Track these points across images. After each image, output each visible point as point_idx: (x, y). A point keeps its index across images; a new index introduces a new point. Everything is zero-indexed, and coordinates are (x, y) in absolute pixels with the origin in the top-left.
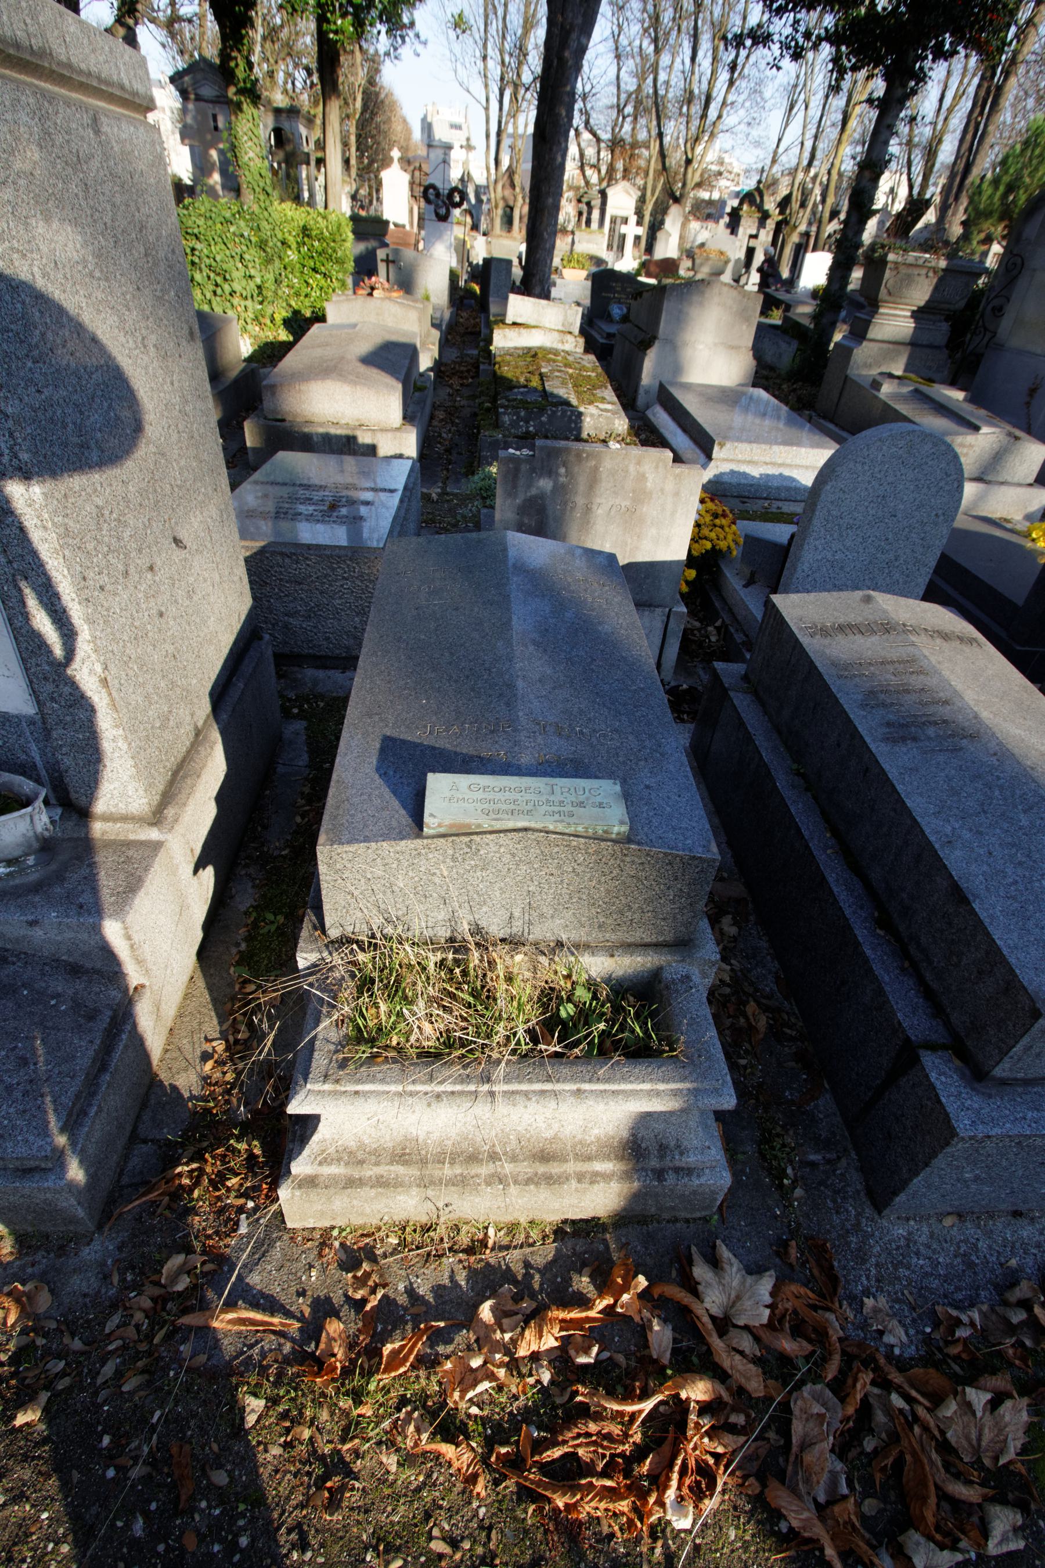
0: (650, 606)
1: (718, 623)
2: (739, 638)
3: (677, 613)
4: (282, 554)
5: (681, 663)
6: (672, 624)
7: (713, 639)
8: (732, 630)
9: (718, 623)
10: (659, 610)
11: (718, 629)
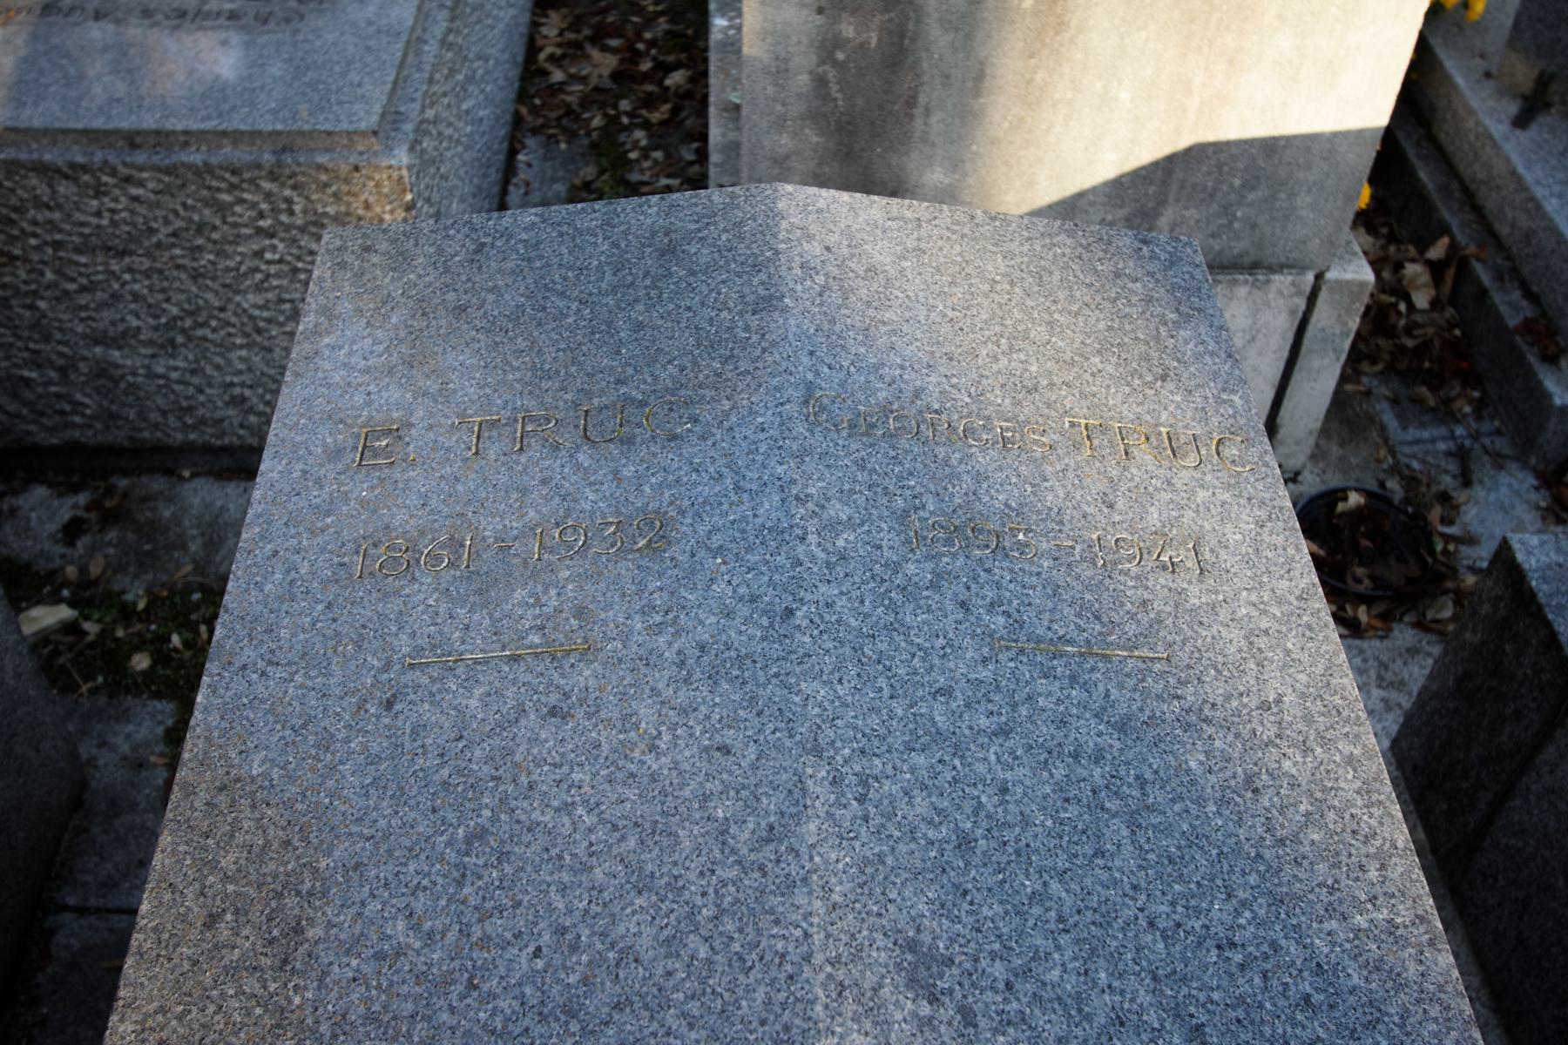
0: (1254, 267)
1: (1437, 252)
2: (1510, 307)
3: (1340, 285)
4: (42, 169)
5: (1345, 413)
6: (1323, 315)
7: (1421, 300)
8: (1485, 276)
9: (1437, 252)
10: (1282, 281)
11: (1436, 269)
